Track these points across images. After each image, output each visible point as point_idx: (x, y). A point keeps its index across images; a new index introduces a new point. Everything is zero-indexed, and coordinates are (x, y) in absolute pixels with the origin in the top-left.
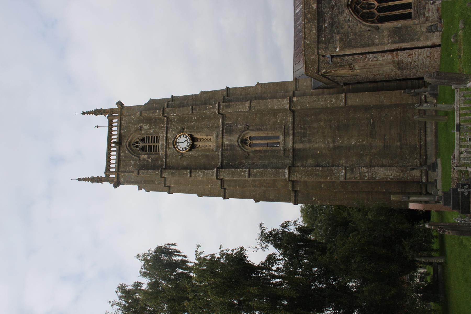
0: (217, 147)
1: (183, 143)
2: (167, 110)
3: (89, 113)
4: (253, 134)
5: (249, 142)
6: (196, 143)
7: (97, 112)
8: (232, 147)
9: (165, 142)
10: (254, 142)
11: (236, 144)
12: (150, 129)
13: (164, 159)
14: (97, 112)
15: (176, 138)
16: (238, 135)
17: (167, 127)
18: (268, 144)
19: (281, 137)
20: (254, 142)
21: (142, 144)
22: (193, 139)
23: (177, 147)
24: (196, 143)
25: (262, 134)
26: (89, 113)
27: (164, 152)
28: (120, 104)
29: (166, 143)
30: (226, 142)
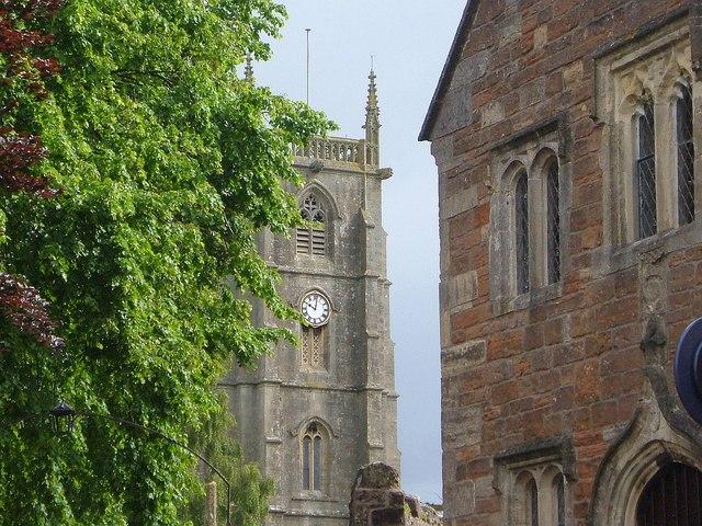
0: (305, 376)
1: (316, 312)
2: (375, 284)
3: (372, 89)
4: (323, 443)
5: (313, 436)
6: (311, 332)
7: (372, 111)
8: (305, 406)
9: (316, 271)
10: (311, 445)
11: (312, 414)
12: (340, 239)
13: (287, 268)
14: (372, 111)
15: (322, 294)
16: (324, 418)
17: (343, 277)
18: (307, 470)
19: (318, 494)
20: (311, 445)
21: (312, 214)
22: (318, 330)
23: (309, 297)
24: (311, 332)
25: (323, 460)
26: (372, 89)
27: (299, 268)
28: (385, 174)
29: (316, 275)
30: (314, 395)
